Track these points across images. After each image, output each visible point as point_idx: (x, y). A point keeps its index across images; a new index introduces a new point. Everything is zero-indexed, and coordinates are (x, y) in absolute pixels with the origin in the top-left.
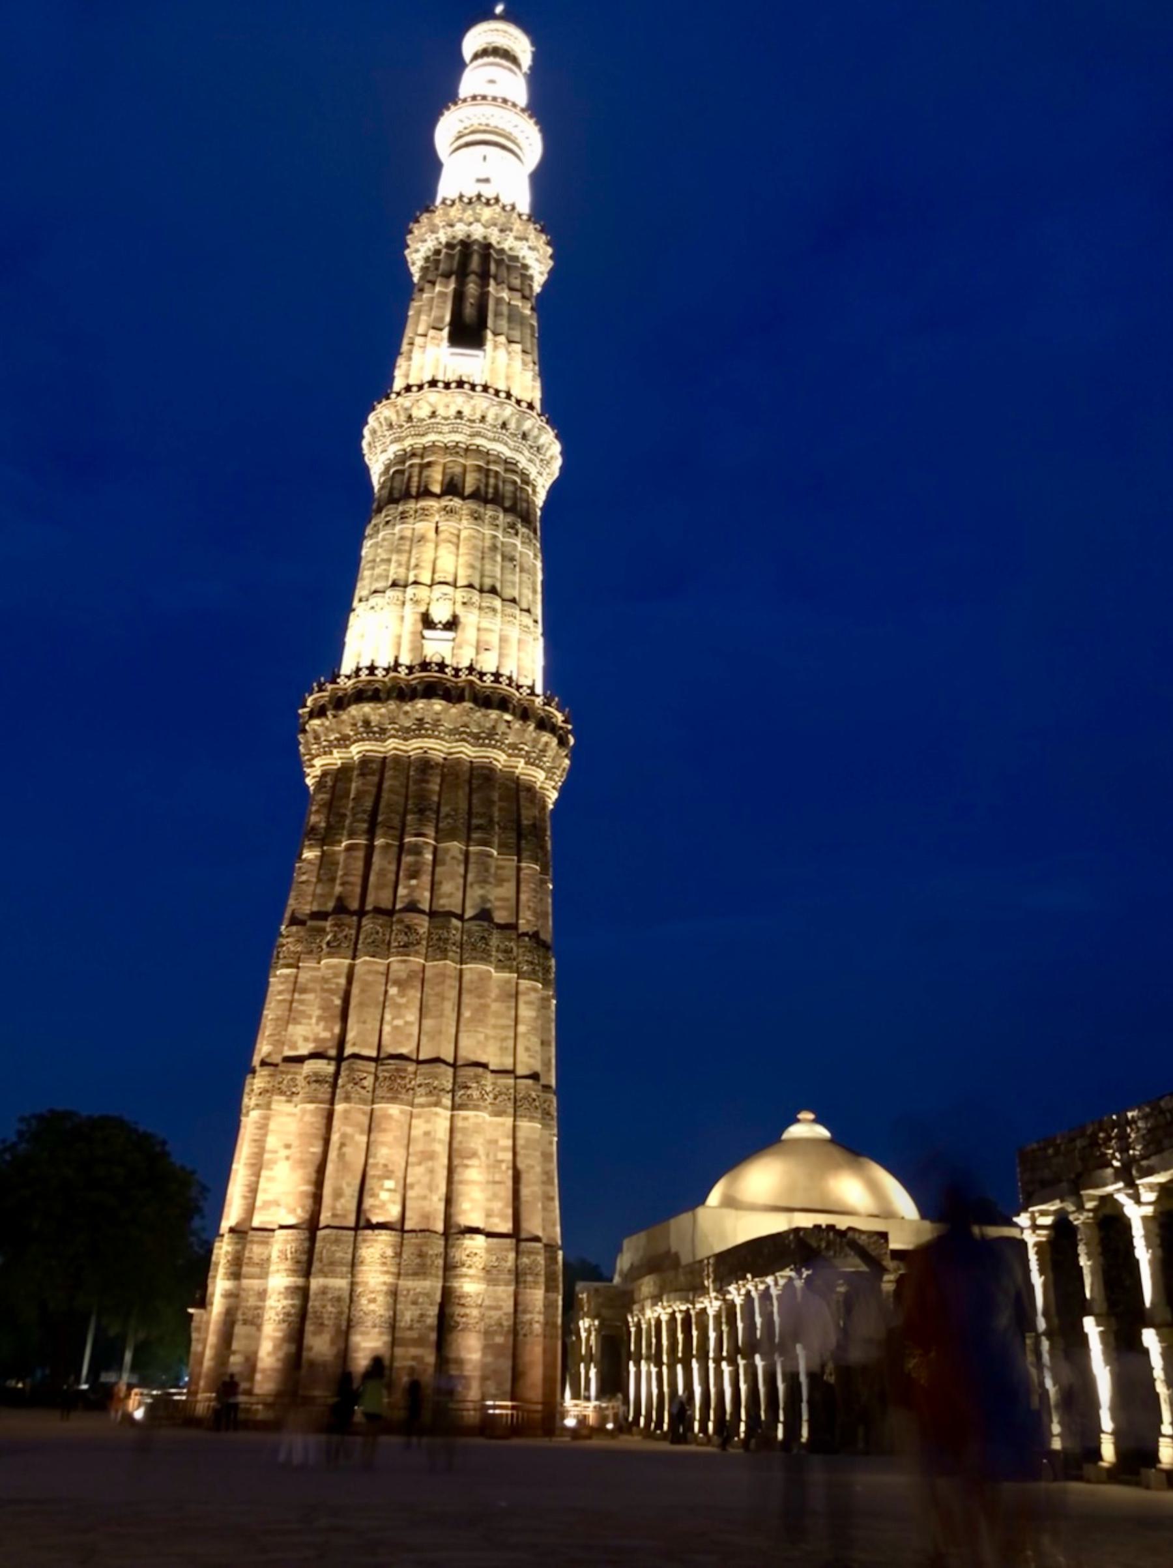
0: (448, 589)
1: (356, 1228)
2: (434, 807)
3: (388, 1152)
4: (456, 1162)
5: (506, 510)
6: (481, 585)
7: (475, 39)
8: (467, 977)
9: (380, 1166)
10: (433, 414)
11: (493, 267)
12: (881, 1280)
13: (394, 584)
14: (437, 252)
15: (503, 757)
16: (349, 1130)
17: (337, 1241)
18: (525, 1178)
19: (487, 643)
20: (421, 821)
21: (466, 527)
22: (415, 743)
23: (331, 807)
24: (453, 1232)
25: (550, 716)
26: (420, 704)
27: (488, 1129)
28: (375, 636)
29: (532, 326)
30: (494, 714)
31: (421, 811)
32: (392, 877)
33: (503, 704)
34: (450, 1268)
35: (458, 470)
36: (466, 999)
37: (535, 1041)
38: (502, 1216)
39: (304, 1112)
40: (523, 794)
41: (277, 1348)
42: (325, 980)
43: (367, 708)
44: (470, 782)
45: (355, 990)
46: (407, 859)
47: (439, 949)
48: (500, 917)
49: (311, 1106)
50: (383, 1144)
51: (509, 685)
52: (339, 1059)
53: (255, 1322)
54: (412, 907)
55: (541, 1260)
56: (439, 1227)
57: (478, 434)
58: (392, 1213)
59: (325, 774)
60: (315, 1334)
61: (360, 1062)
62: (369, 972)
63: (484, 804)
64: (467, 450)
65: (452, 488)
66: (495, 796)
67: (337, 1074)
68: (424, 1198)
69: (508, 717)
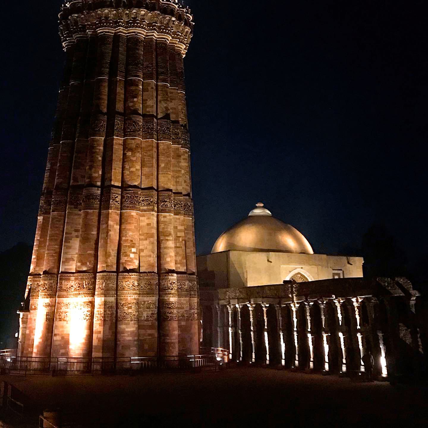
1: (118, 272)
3: (132, 234)
4: (162, 238)
8: (161, 147)
9: (129, 241)
12: (410, 300)
15: (156, 35)
22: (132, 30)
36: (161, 158)
47: (148, 134)
48: (173, 117)
50: (129, 230)
58: (134, 265)
61: (114, 189)
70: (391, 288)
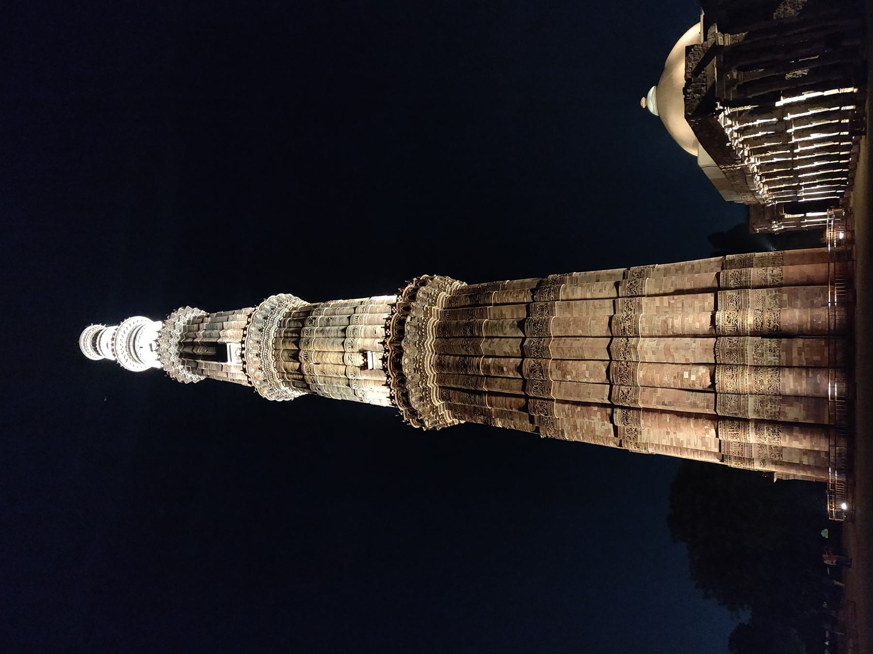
0: (346, 356)
2: (462, 358)
3: (666, 376)
5: (304, 326)
6: (342, 337)
7: (90, 355)
10: (260, 369)
11: (190, 340)
13: (349, 385)
14: (188, 369)
16: (654, 400)
17: (724, 405)
18: (679, 287)
19: (372, 332)
20: (471, 366)
21: (314, 348)
23: (474, 411)
24: (714, 332)
25: (408, 293)
26: (406, 371)
27: (650, 313)
28: (376, 394)
29: (217, 316)
30: (407, 328)
31: (465, 366)
32: (504, 380)
33: (401, 322)
34: (738, 333)
35: (286, 354)
37: (596, 286)
38: (704, 300)
39: (645, 425)
40: (453, 305)
41: (797, 439)
42: (567, 416)
43: (413, 400)
44: (448, 338)
45: (572, 399)
46: (493, 373)
47: (542, 352)
49: (642, 422)
51: (391, 319)
52: (612, 406)
53: (780, 450)
54: (519, 369)
55: (731, 272)
56: (712, 341)
57: (266, 344)
59: (455, 417)
60: (785, 416)
61: (613, 395)
62: (559, 391)
63: (459, 329)
64: (276, 349)
65: (295, 356)
66: (454, 322)
67: (622, 407)
68: (694, 352)
69: (409, 319)
70: (703, 86)
